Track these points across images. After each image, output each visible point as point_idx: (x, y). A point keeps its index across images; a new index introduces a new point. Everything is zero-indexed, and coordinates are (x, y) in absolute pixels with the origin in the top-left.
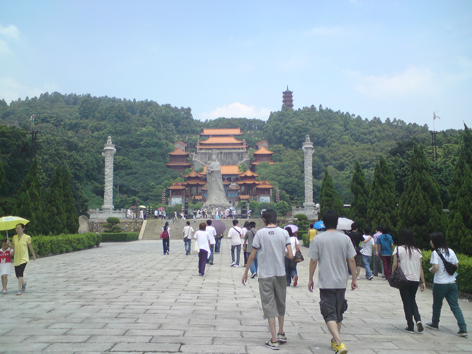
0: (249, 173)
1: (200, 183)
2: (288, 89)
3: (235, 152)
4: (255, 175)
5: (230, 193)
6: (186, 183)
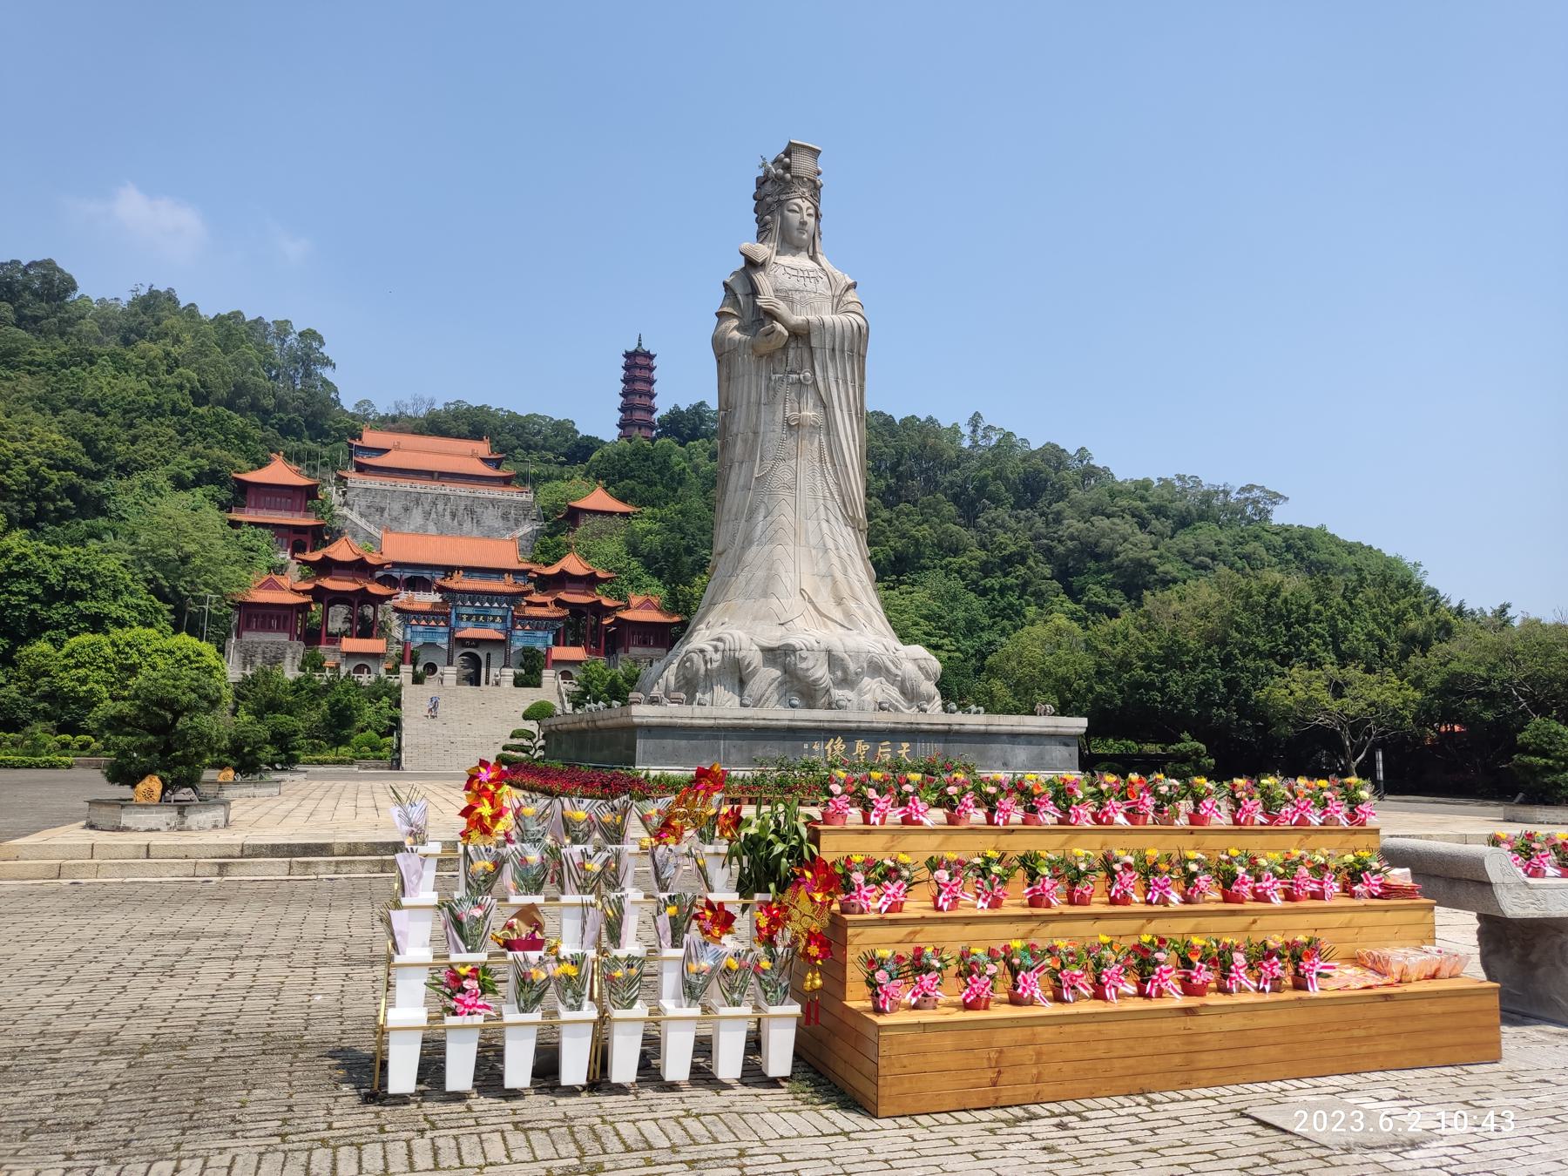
0: (573, 564)
1: (375, 589)
2: (640, 345)
3: (494, 502)
4: (600, 574)
5: (523, 629)
6: (310, 586)
